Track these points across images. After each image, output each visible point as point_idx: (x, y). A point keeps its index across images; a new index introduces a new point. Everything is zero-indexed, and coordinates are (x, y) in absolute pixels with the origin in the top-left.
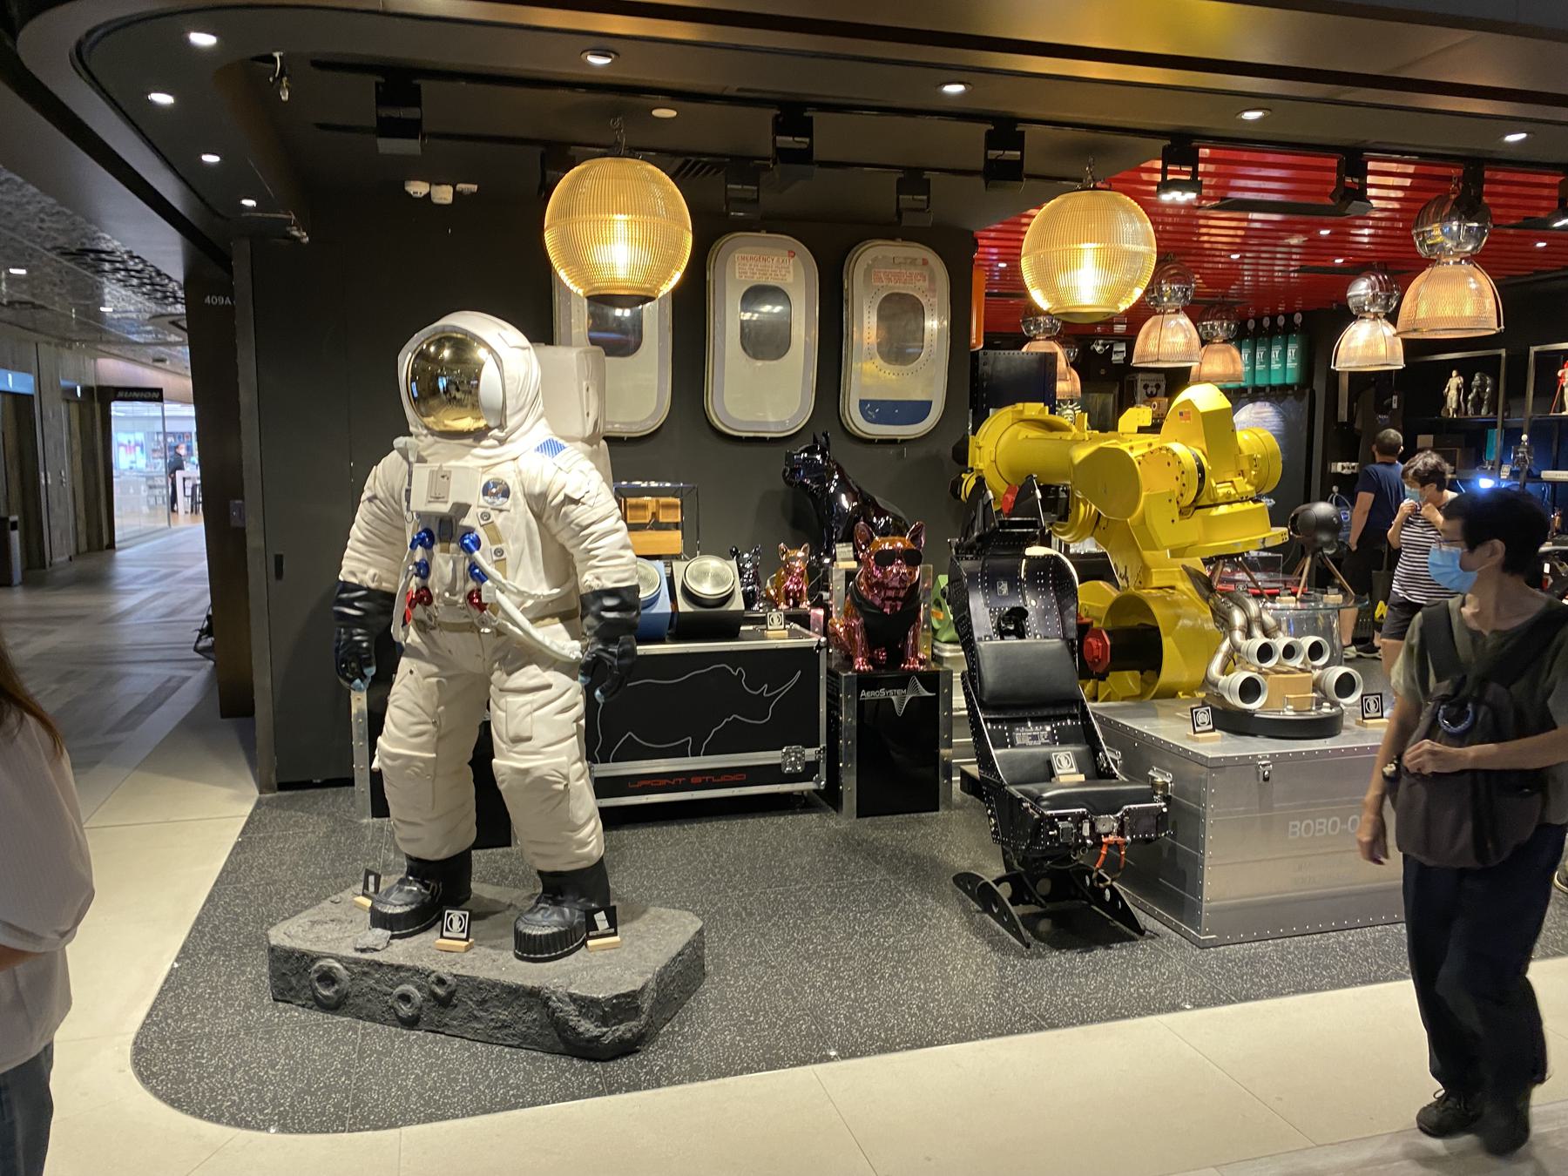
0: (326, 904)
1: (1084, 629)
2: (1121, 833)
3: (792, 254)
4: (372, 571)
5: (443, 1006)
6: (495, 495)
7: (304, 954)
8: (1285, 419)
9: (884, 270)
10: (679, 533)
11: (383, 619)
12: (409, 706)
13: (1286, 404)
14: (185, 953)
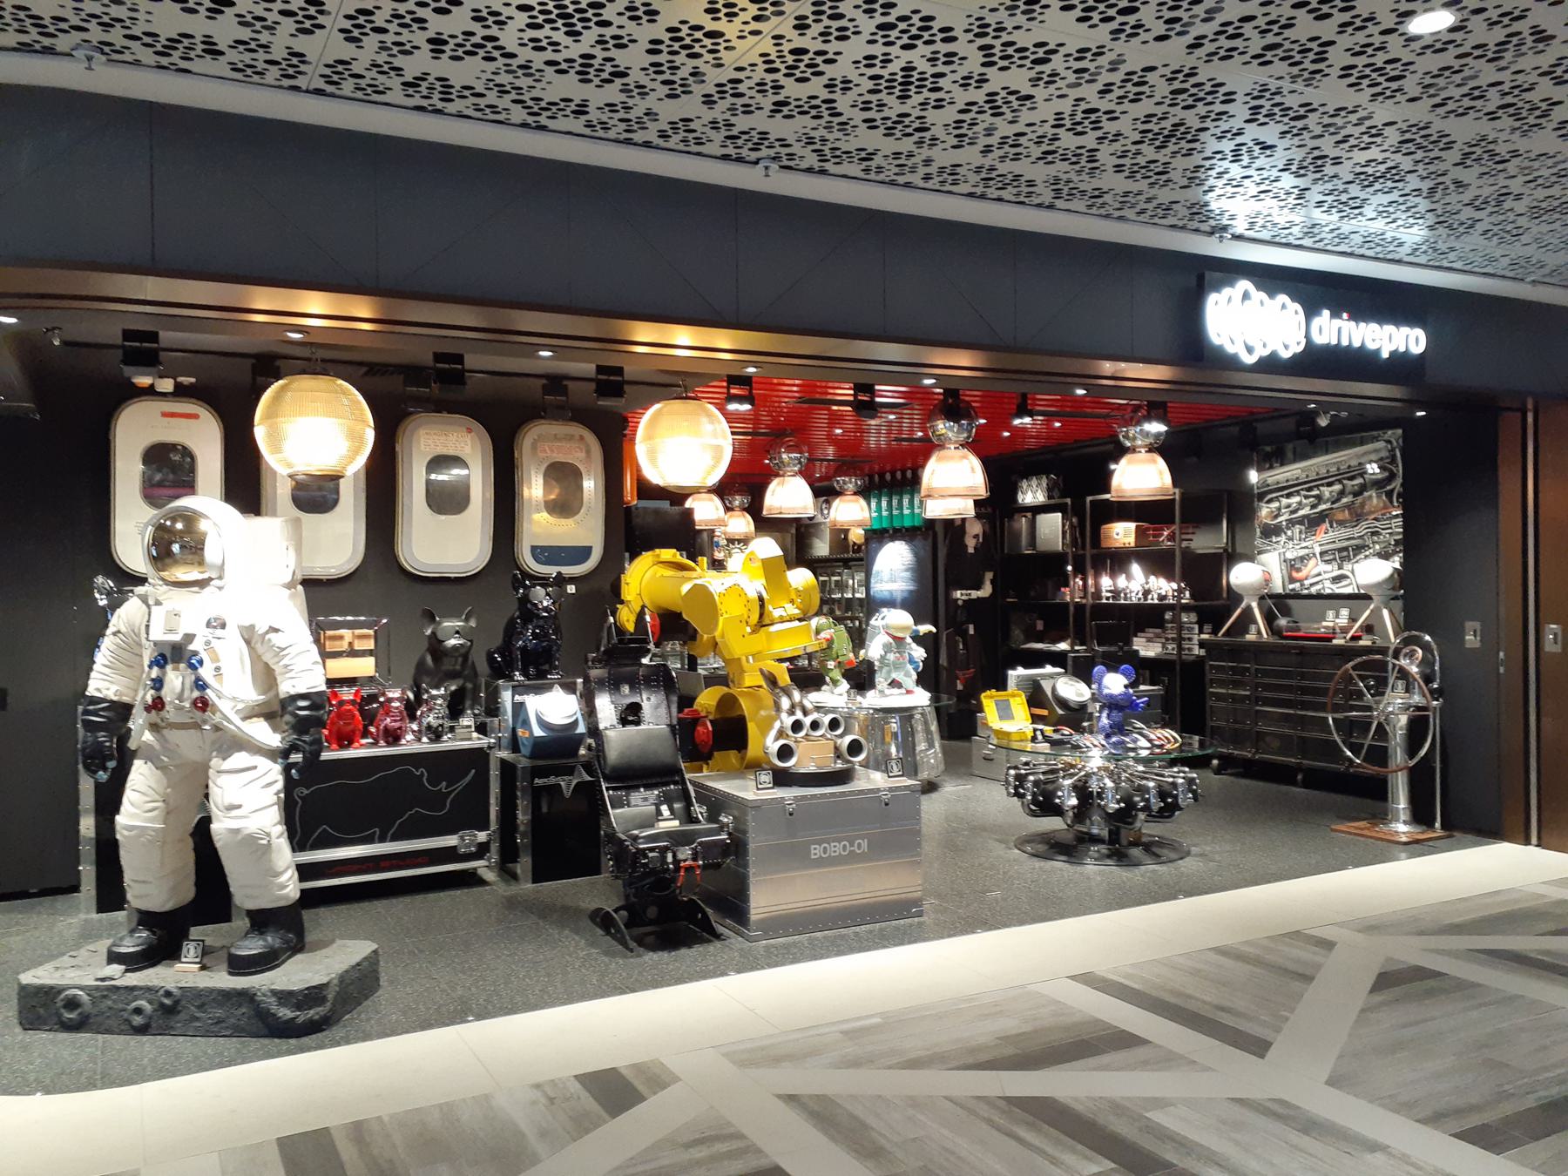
1: (696, 720)
2: (695, 859)
3: (469, 430)
4: (114, 688)
5: (169, 1014)
8: (916, 555)
9: (545, 445)
10: (372, 660)
13: (916, 542)
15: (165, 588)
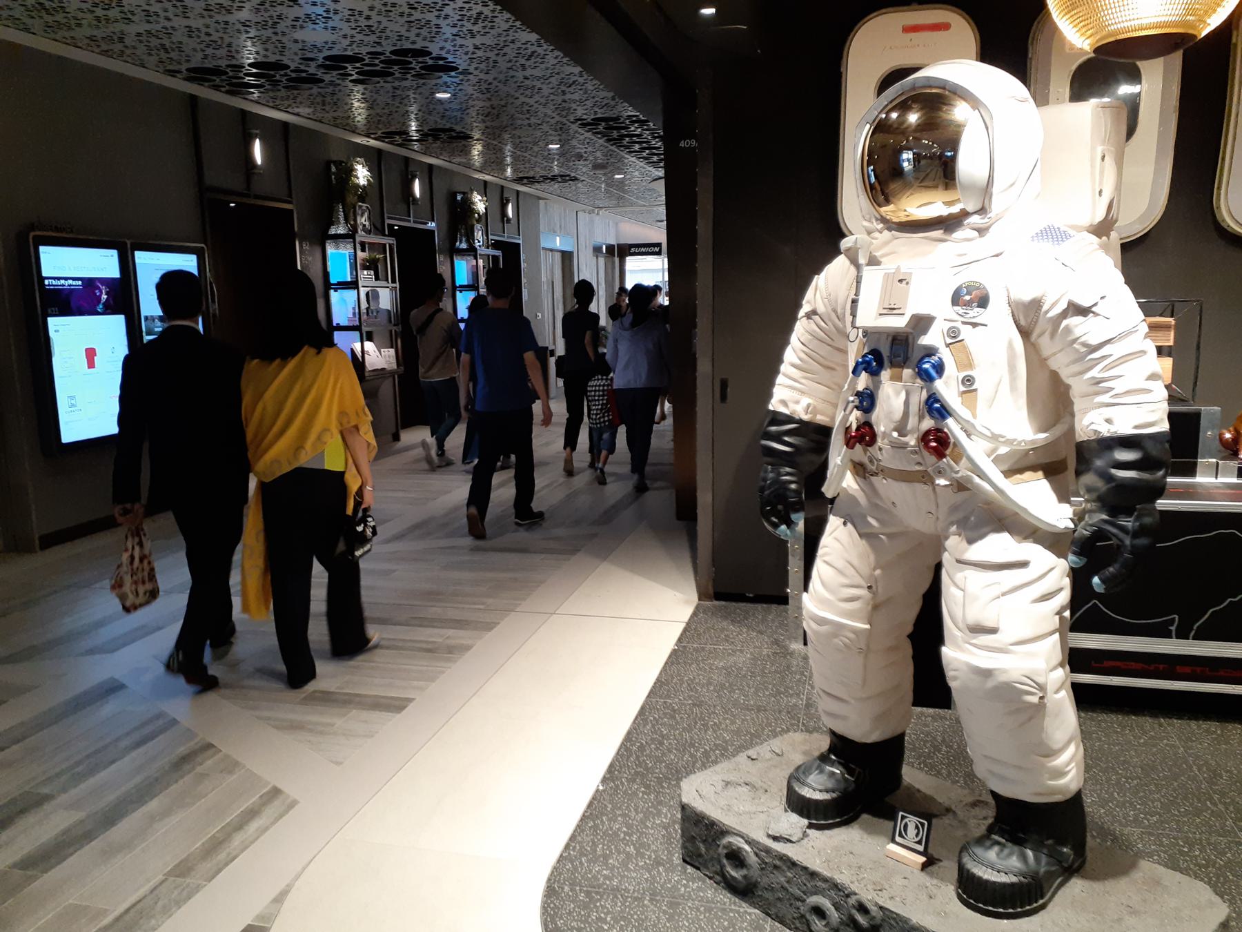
0: (742, 758)
4: (805, 401)
6: (968, 304)
7: (712, 824)
11: (818, 460)
12: (840, 564)
14: (611, 775)
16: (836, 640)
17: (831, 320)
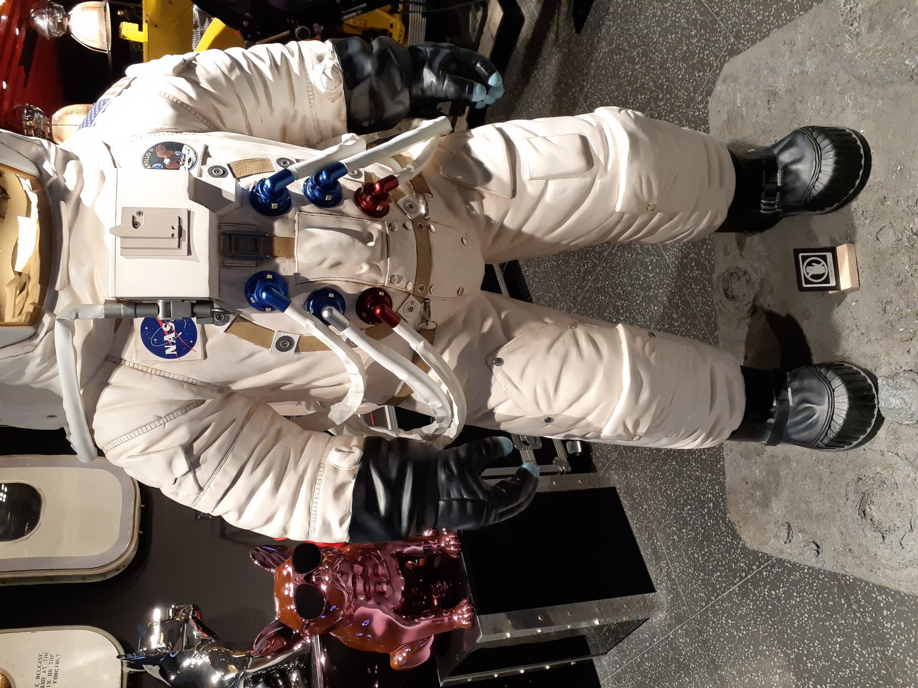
12: (553, 362)
15: (63, 303)
16: (652, 359)
17: (200, 418)
